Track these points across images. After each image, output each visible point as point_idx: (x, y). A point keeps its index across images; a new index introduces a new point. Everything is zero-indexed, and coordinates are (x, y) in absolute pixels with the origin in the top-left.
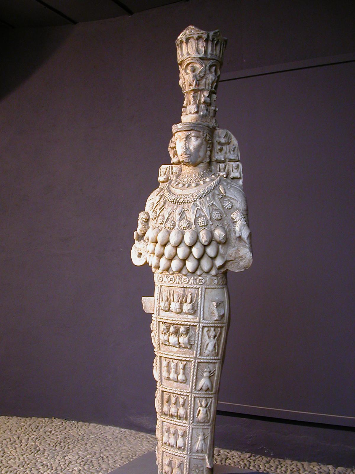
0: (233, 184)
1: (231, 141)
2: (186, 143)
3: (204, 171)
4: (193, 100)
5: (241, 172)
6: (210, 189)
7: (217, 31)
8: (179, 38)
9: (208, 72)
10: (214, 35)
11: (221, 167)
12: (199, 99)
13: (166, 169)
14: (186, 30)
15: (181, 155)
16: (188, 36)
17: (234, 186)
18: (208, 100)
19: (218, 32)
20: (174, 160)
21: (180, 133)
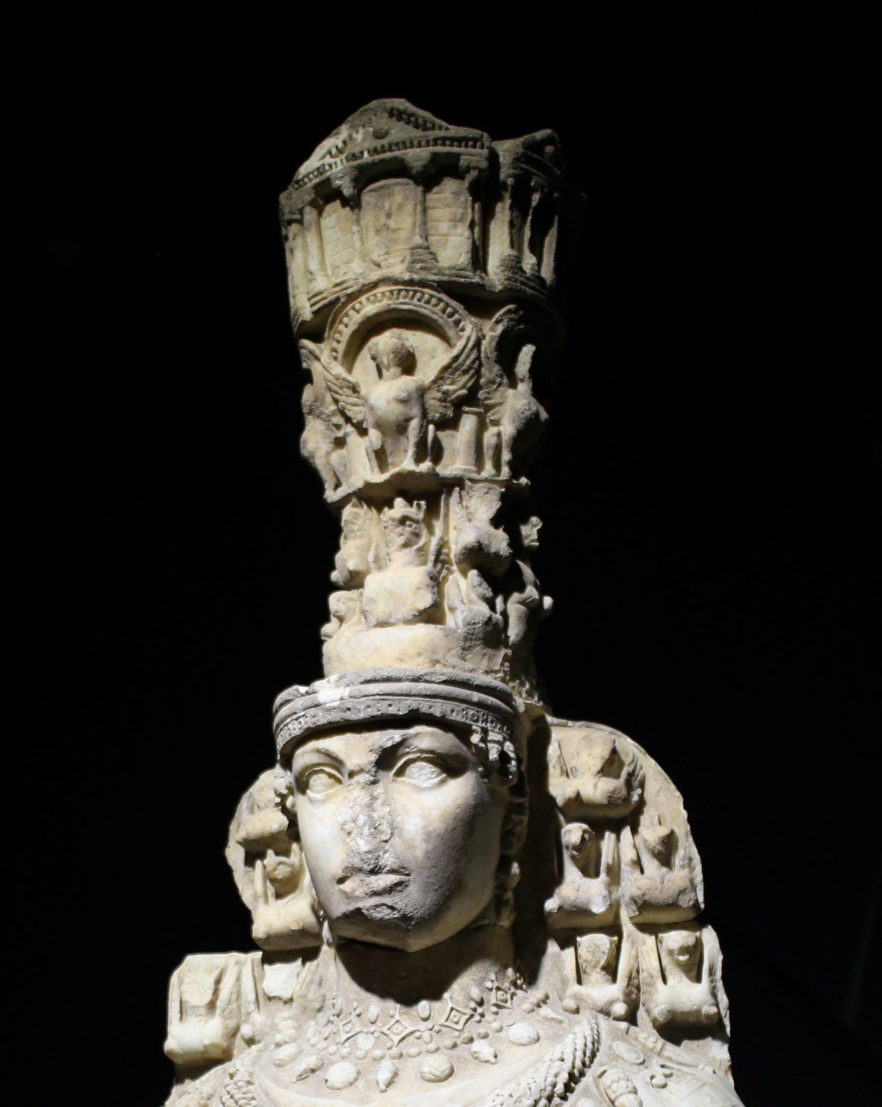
0: (680, 1059)
1: (641, 797)
2: (374, 798)
3: (484, 979)
4: (401, 540)
5: (720, 984)
6: (547, 1093)
7: (539, 135)
8: (305, 169)
9: (491, 371)
10: (524, 155)
11: (582, 951)
12: (442, 539)
13: (218, 982)
14: (354, 127)
15: (340, 874)
16: (366, 155)
17: (684, 1069)
18: (499, 542)
19: (548, 141)
20: (270, 917)
21: (334, 744)
